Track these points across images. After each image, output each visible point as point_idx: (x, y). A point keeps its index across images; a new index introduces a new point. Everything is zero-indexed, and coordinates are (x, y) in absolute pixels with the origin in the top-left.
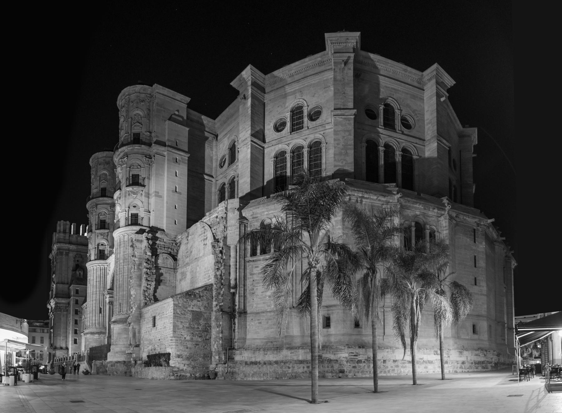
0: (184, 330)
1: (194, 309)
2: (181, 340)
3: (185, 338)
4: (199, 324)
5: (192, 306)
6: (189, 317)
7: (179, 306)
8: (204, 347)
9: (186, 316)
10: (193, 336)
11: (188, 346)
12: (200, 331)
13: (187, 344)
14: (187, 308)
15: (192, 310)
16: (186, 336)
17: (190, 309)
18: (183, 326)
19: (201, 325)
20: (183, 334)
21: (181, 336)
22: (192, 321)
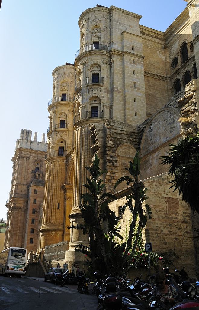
0: (160, 220)
1: (169, 196)
2: (157, 233)
3: (162, 231)
4: (177, 214)
5: (166, 192)
6: (164, 205)
7: (152, 193)
8: (185, 242)
9: (160, 204)
10: (171, 228)
11: (166, 241)
12: (179, 222)
13: (164, 238)
14: (161, 194)
15: (167, 196)
16: (162, 228)
17: (164, 195)
18: (159, 216)
19: (179, 214)
20: (159, 225)
21: (157, 228)
22: (168, 210)
